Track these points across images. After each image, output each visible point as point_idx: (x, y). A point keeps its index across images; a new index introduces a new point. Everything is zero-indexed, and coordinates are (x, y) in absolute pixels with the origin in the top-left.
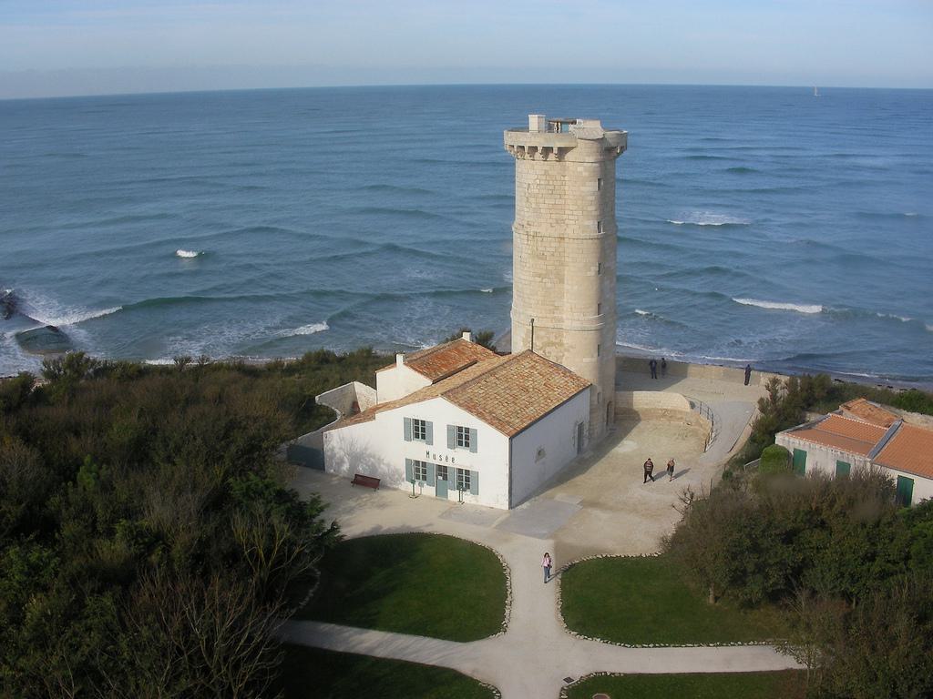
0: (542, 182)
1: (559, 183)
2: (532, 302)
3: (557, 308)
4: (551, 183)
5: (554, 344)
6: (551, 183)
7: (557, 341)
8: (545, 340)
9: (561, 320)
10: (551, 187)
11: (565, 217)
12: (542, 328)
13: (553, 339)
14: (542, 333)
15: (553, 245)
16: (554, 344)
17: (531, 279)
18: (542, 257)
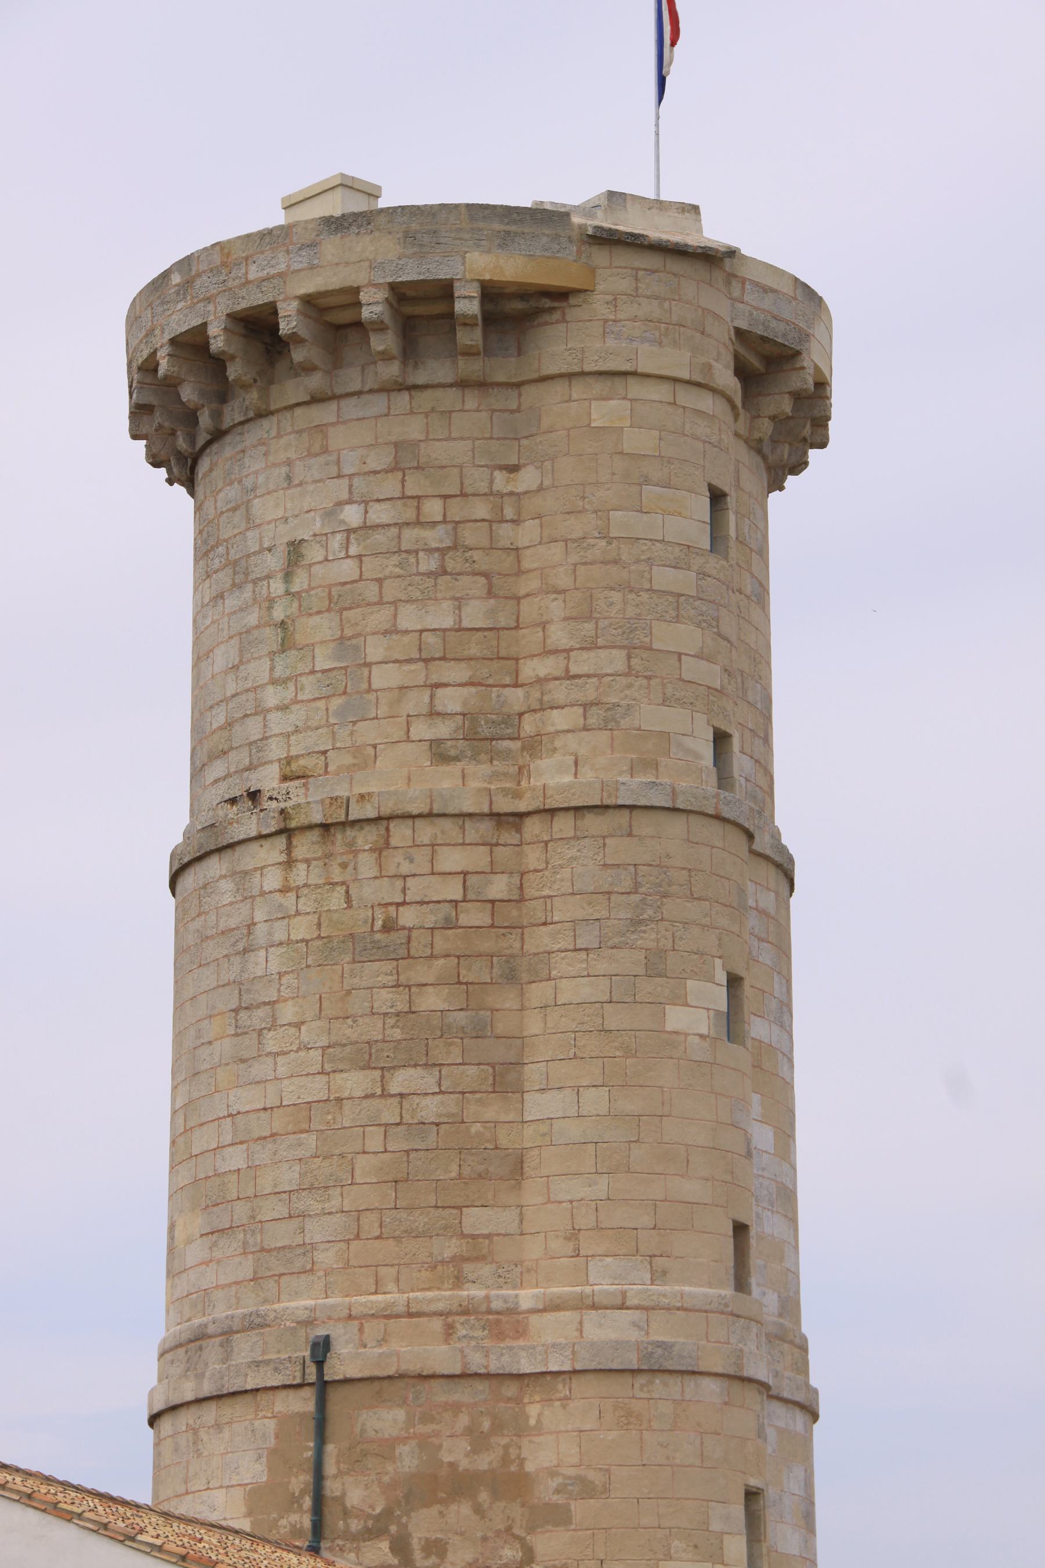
0: (380, 514)
1: (481, 510)
2: (316, 1231)
3: (479, 1249)
4: (433, 509)
5: (460, 1485)
6: (433, 509)
7: (484, 1462)
8: (408, 1460)
9: (506, 1323)
10: (437, 537)
11: (516, 698)
12: (380, 1385)
13: (456, 1452)
14: (386, 1420)
15: (452, 859)
16: (460, 1485)
17: (316, 1089)
18: (386, 939)
